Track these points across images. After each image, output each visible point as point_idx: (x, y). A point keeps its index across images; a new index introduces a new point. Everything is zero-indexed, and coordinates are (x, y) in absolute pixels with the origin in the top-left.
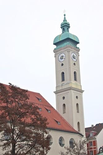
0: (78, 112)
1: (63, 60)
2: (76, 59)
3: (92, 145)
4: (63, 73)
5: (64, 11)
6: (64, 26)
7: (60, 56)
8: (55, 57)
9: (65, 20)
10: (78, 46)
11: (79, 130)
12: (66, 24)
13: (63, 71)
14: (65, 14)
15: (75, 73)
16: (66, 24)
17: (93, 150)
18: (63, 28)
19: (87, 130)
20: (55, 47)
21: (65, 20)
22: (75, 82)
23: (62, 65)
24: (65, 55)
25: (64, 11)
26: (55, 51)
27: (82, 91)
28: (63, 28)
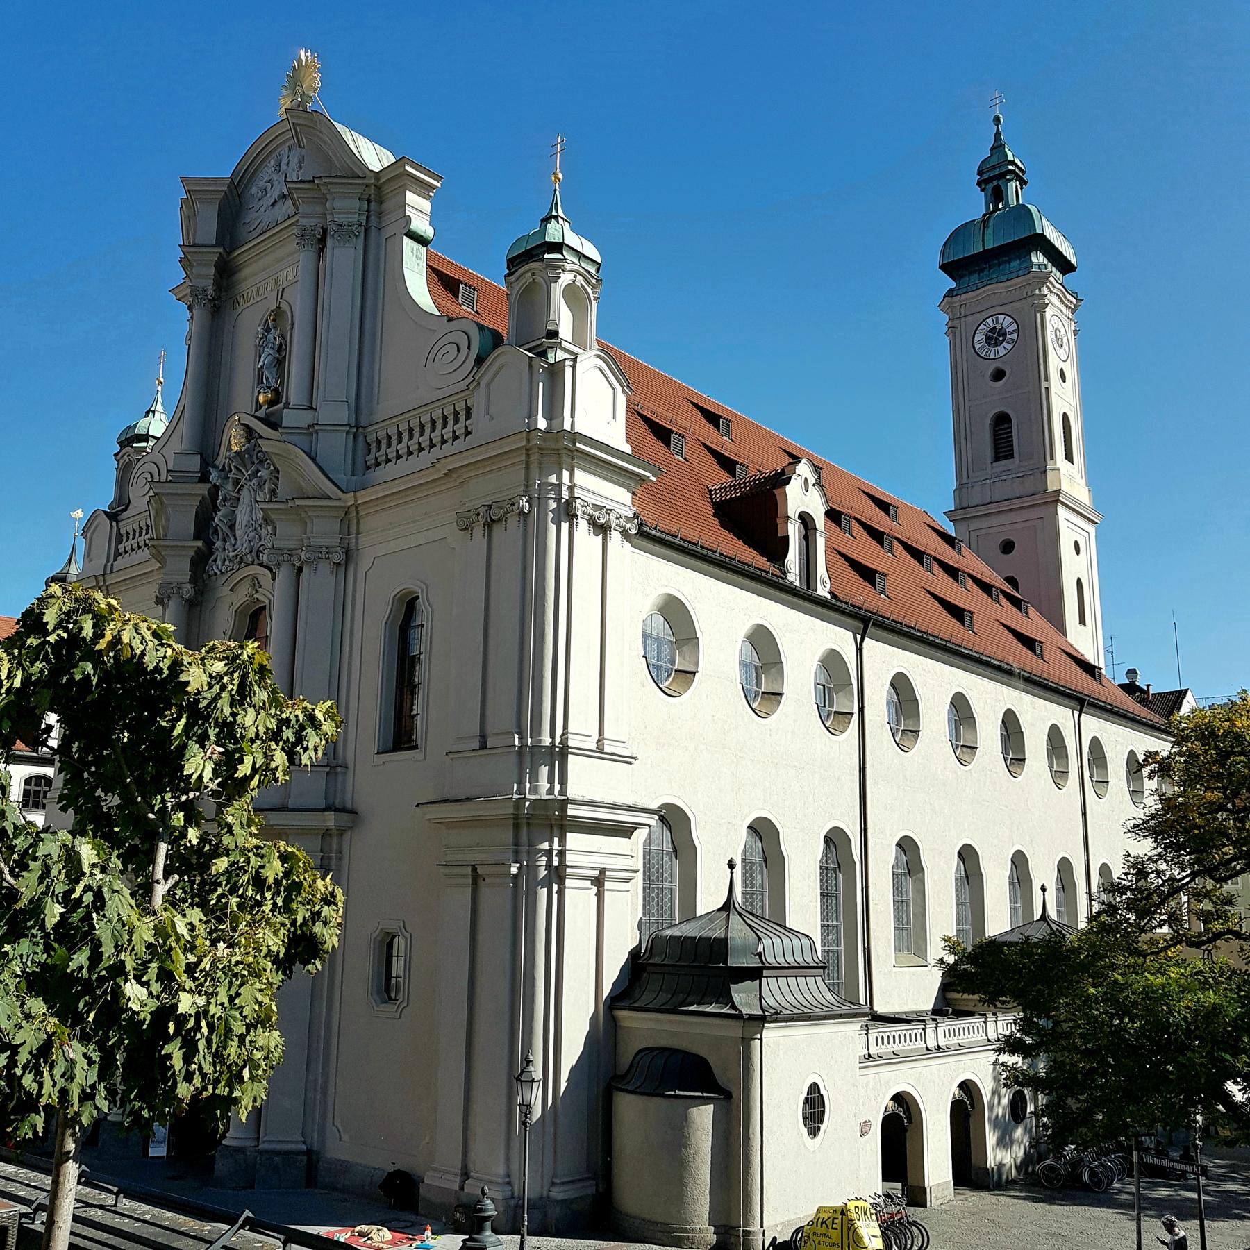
0: (1082, 621)
4: (1002, 421)
8: (952, 329)
9: (998, 147)
12: (1010, 167)
16: (1010, 167)
18: (991, 186)
23: (999, 375)
24: (1014, 326)
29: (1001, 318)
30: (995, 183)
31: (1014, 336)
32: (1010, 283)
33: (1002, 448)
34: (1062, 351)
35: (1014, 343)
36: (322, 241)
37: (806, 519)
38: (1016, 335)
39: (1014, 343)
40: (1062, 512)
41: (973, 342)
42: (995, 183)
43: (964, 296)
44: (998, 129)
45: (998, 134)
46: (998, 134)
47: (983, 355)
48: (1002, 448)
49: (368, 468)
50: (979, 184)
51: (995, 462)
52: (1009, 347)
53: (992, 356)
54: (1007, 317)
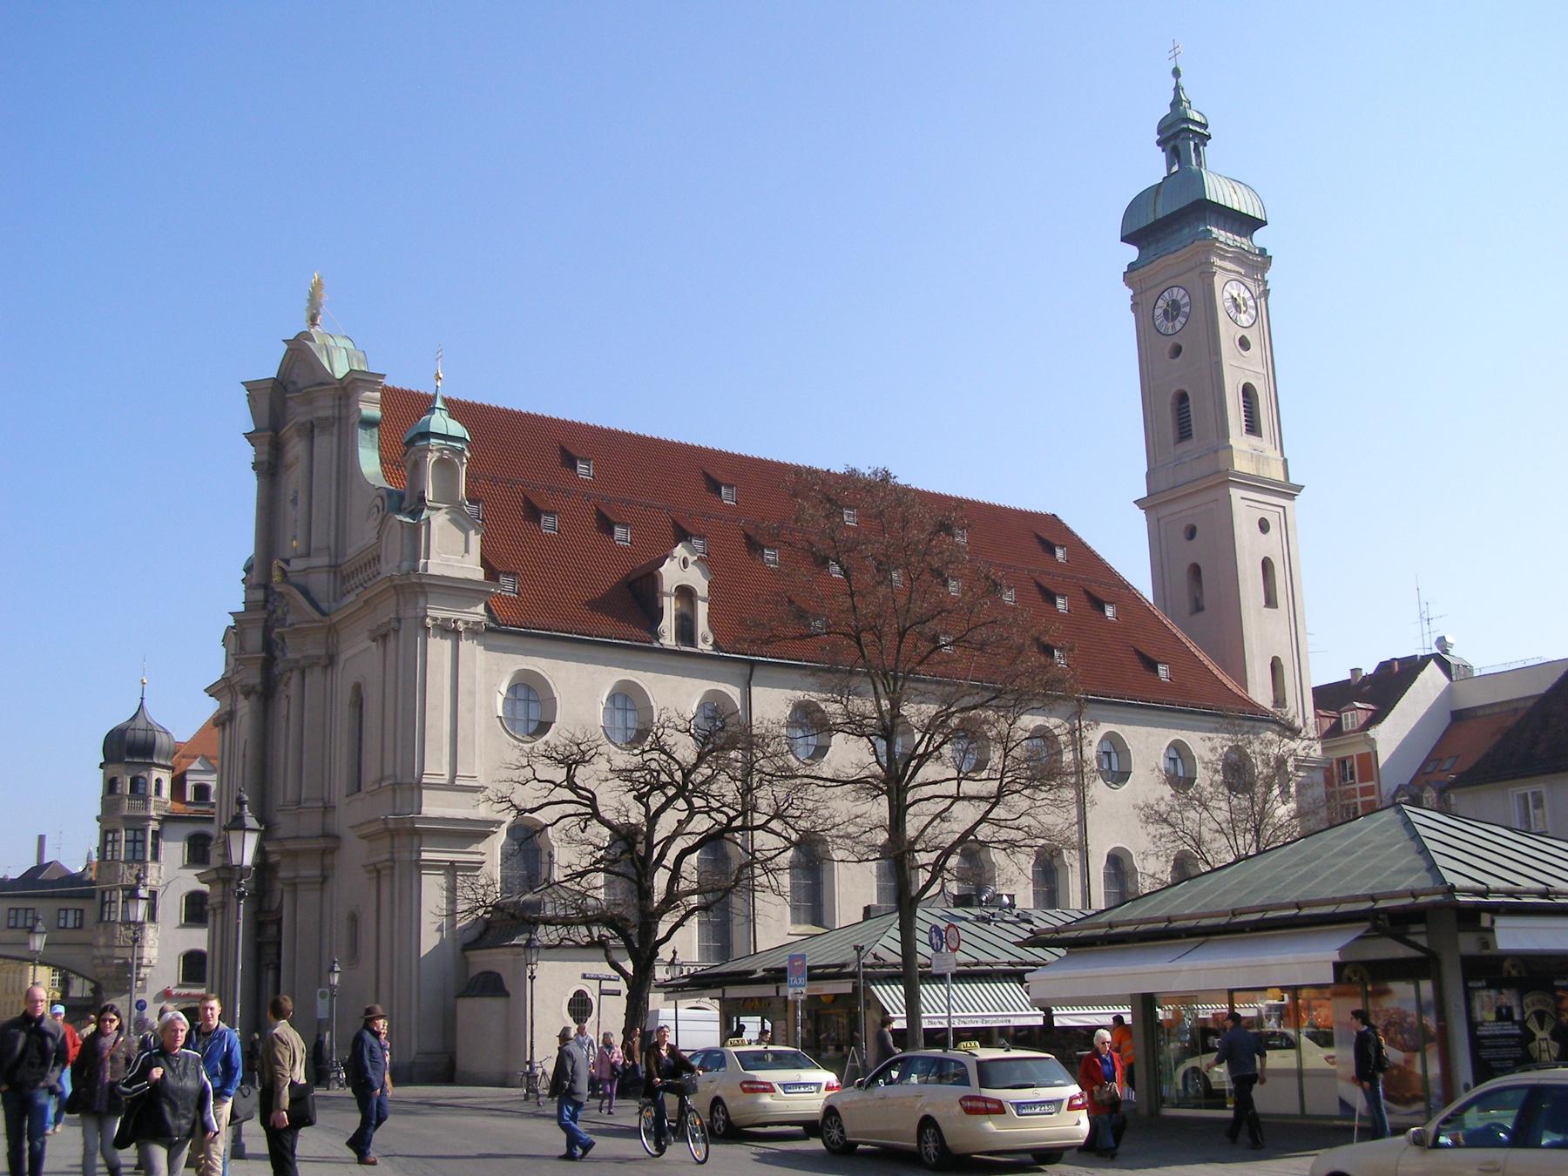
1: (1178, 327)
2: (1254, 313)
3: (1352, 777)
4: (1182, 398)
6: (1175, 136)
7: (1160, 302)
8: (1135, 307)
9: (1177, 102)
10: (1260, 238)
11: (1279, 701)
13: (1174, 390)
17: (1359, 800)
18: (1169, 147)
19: (1330, 697)
22: (1253, 440)
23: (1177, 351)
24: (1186, 299)
27: (1289, 491)
28: (1169, 147)
29: (1175, 289)
30: (1172, 143)
31: (1187, 309)
32: (1179, 253)
33: (1184, 431)
36: (312, 431)
37: (685, 593)
38: (1188, 308)
40: (1236, 494)
41: (1153, 316)
42: (1172, 143)
43: (1142, 270)
46: (1177, 89)
48: (1184, 431)
49: (344, 595)
50: (1159, 143)
51: (1179, 442)
53: (1170, 332)
54: (1181, 290)
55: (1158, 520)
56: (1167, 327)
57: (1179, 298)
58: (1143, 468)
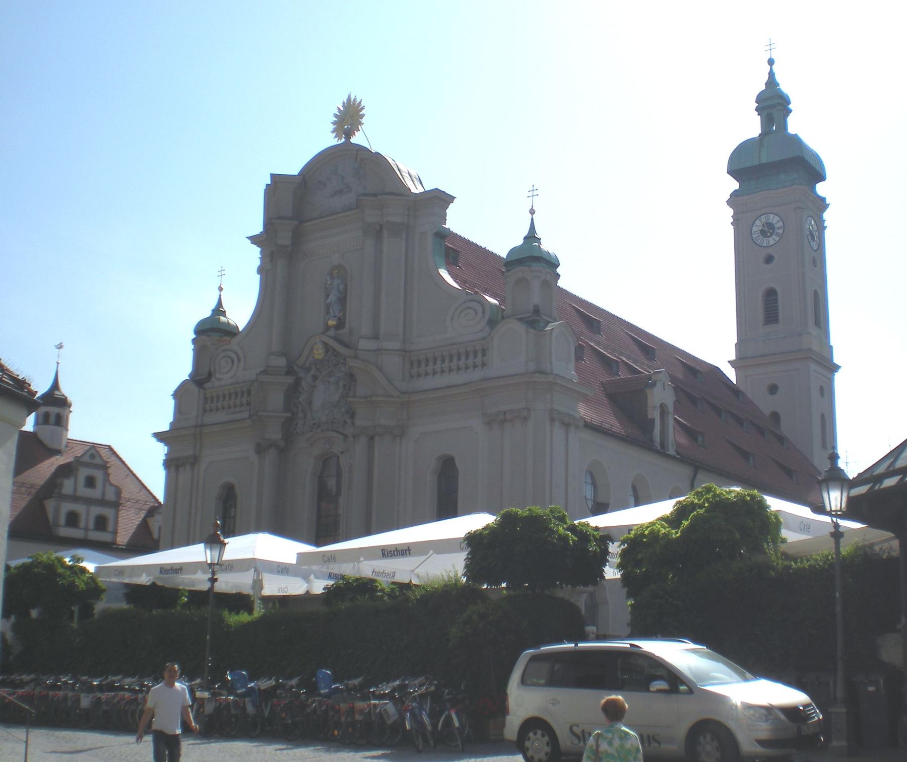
4: (771, 295)
5: (770, 47)
6: (773, 107)
7: (758, 223)
8: (736, 222)
9: (772, 82)
14: (772, 57)
15: (816, 293)
20: (735, 185)
21: (772, 82)
23: (769, 259)
24: (780, 224)
25: (770, 47)
26: (734, 200)
29: (771, 216)
34: (815, 243)
35: (781, 236)
37: (663, 407)
39: (781, 236)
44: (771, 69)
45: (771, 74)
46: (771, 74)
47: (758, 243)
49: (412, 377)
52: (777, 238)
53: (765, 244)
54: (776, 217)
55: (746, 377)
56: (761, 240)
57: (774, 222)
58: (734, 339)
